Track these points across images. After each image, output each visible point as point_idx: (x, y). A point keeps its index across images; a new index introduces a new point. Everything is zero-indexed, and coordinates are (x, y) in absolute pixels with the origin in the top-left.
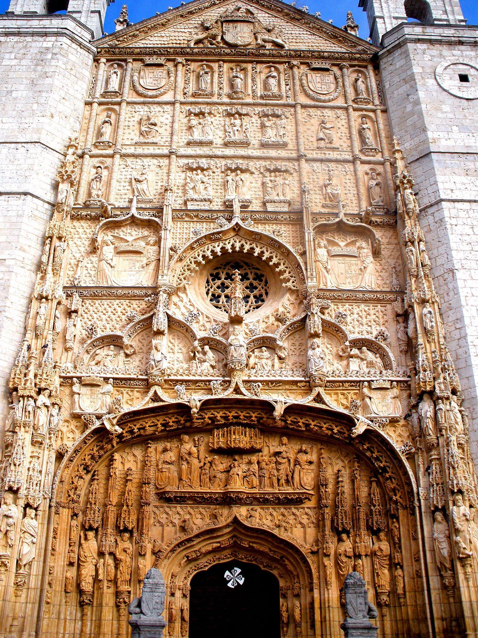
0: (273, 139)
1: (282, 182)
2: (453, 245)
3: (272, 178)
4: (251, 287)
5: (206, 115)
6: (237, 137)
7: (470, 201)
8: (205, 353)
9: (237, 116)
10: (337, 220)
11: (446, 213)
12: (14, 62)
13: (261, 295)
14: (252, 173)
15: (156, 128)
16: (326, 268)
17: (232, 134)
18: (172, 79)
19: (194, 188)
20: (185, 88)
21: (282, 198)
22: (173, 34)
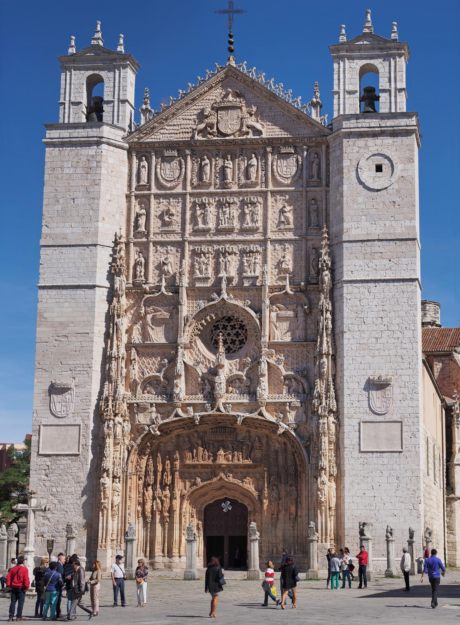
0: (250, 225)
1: (253, 261)
2: (345, 314)
3: (248, 259)
4: (237, 334)
5: (207, 205)
6: (227, 225)
7: (362, 281)
8: (206, 384)
9: (227, 205)
10: (284, 291)
11: (345, 291)
12: (71, 171)
13: (243, 339)
14: (235, 254)
15: (175, 218)
16: (275, 326)
17: (223, 223)
18: (184, 170)
19: (199, 269)
20: (192, 179)
21: (253, 274)
22: (183, 122)
